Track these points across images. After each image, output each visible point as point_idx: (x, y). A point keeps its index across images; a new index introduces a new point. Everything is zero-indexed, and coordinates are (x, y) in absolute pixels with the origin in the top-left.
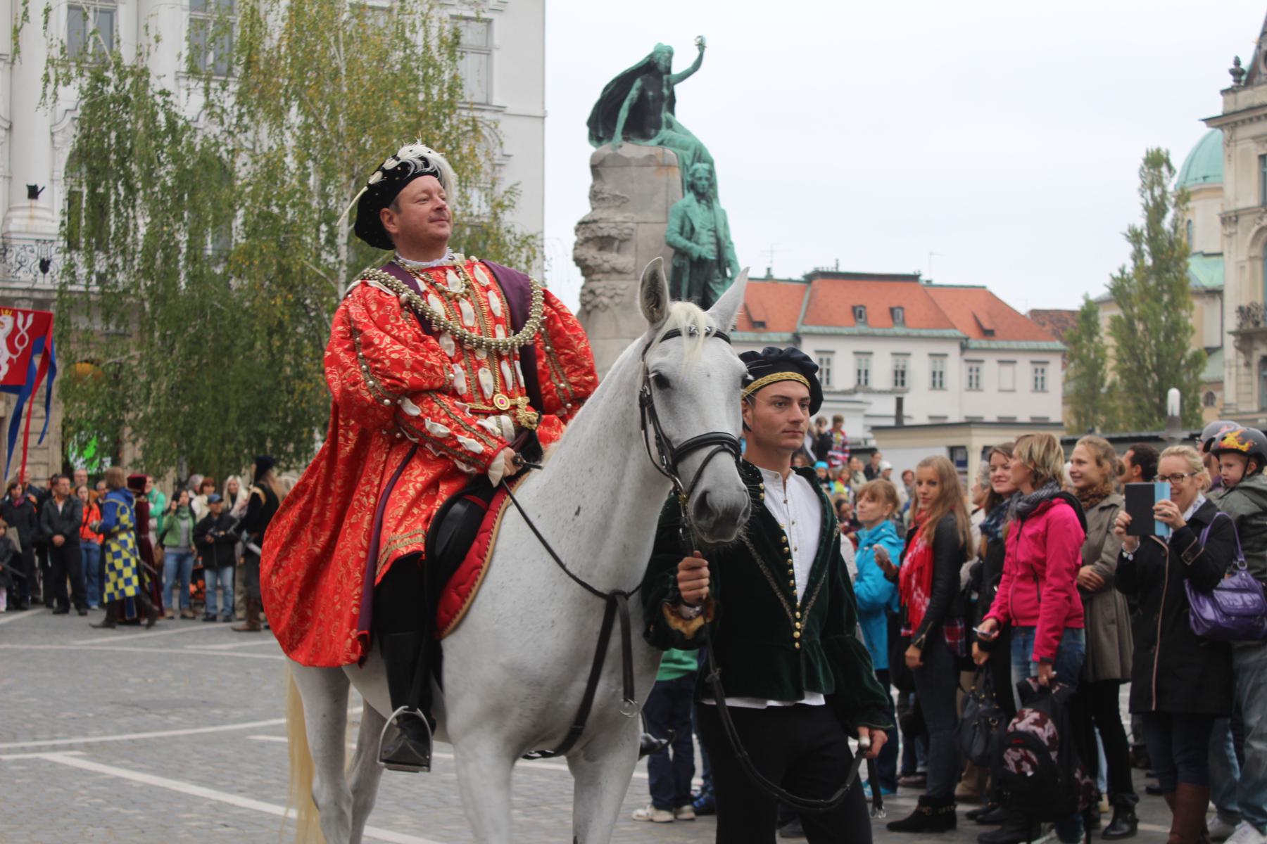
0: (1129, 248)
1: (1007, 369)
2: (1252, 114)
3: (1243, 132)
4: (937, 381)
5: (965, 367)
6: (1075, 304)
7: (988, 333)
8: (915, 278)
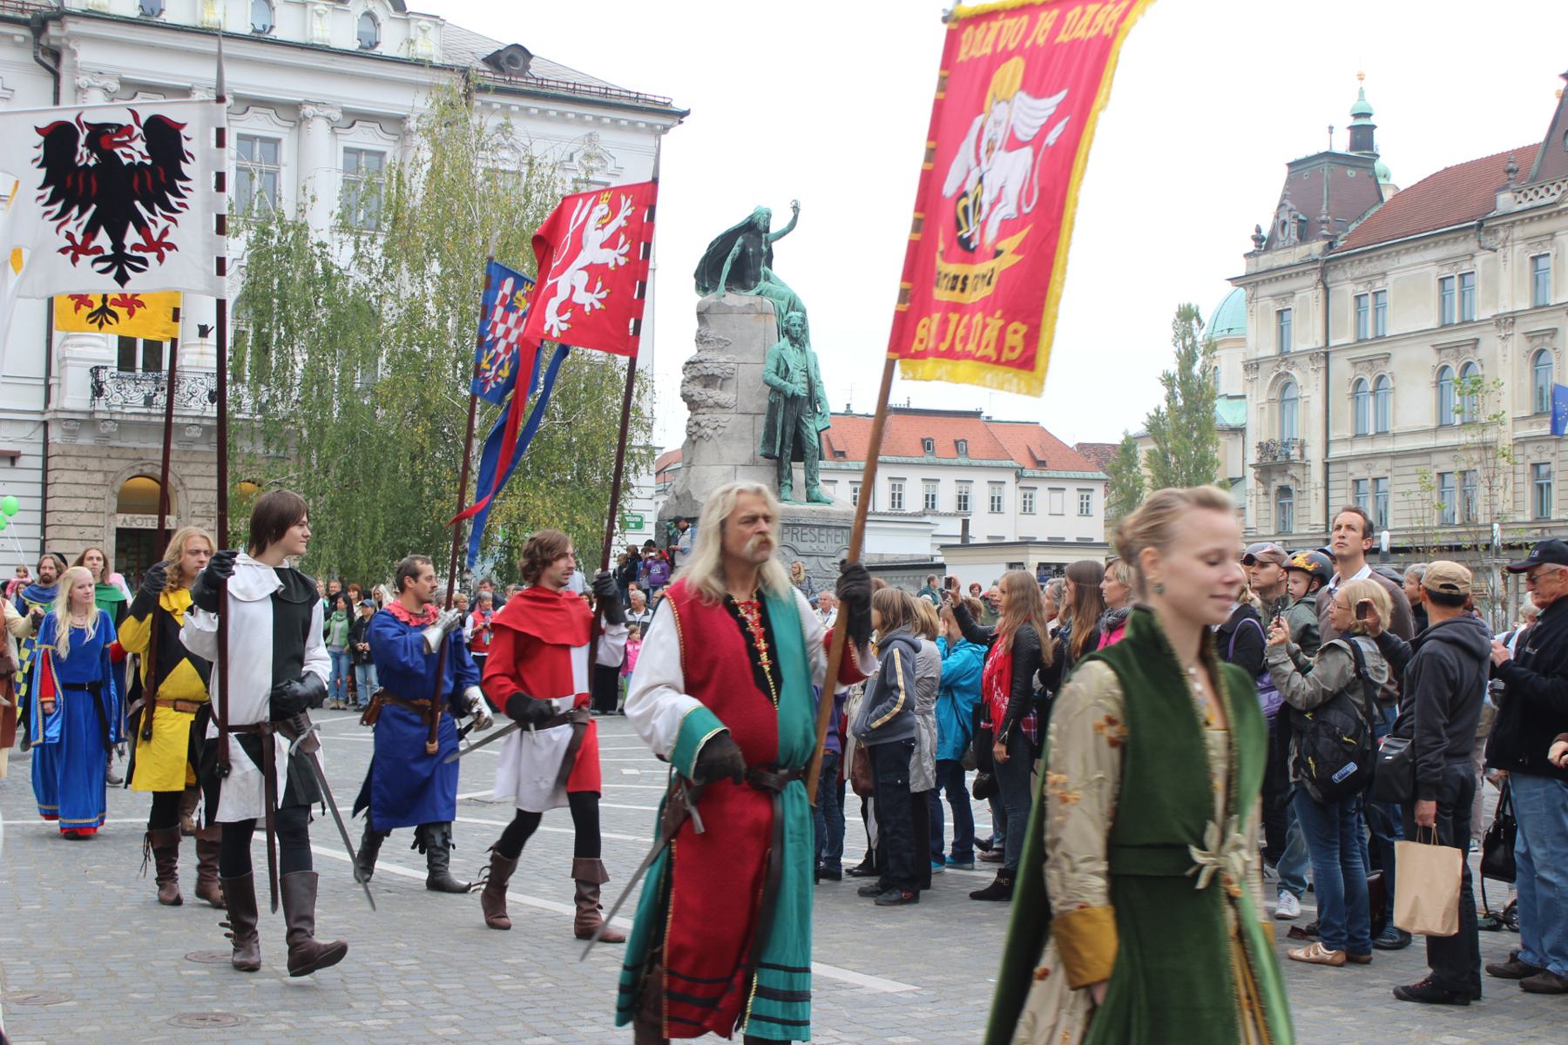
0: (1164, 391)
1: (1058, 495)
3: (1264, 291)
4: (996, 505)
5: (1020, 493)
6: (1117, 439)
7: (1041, 464)
8: (977, 414)
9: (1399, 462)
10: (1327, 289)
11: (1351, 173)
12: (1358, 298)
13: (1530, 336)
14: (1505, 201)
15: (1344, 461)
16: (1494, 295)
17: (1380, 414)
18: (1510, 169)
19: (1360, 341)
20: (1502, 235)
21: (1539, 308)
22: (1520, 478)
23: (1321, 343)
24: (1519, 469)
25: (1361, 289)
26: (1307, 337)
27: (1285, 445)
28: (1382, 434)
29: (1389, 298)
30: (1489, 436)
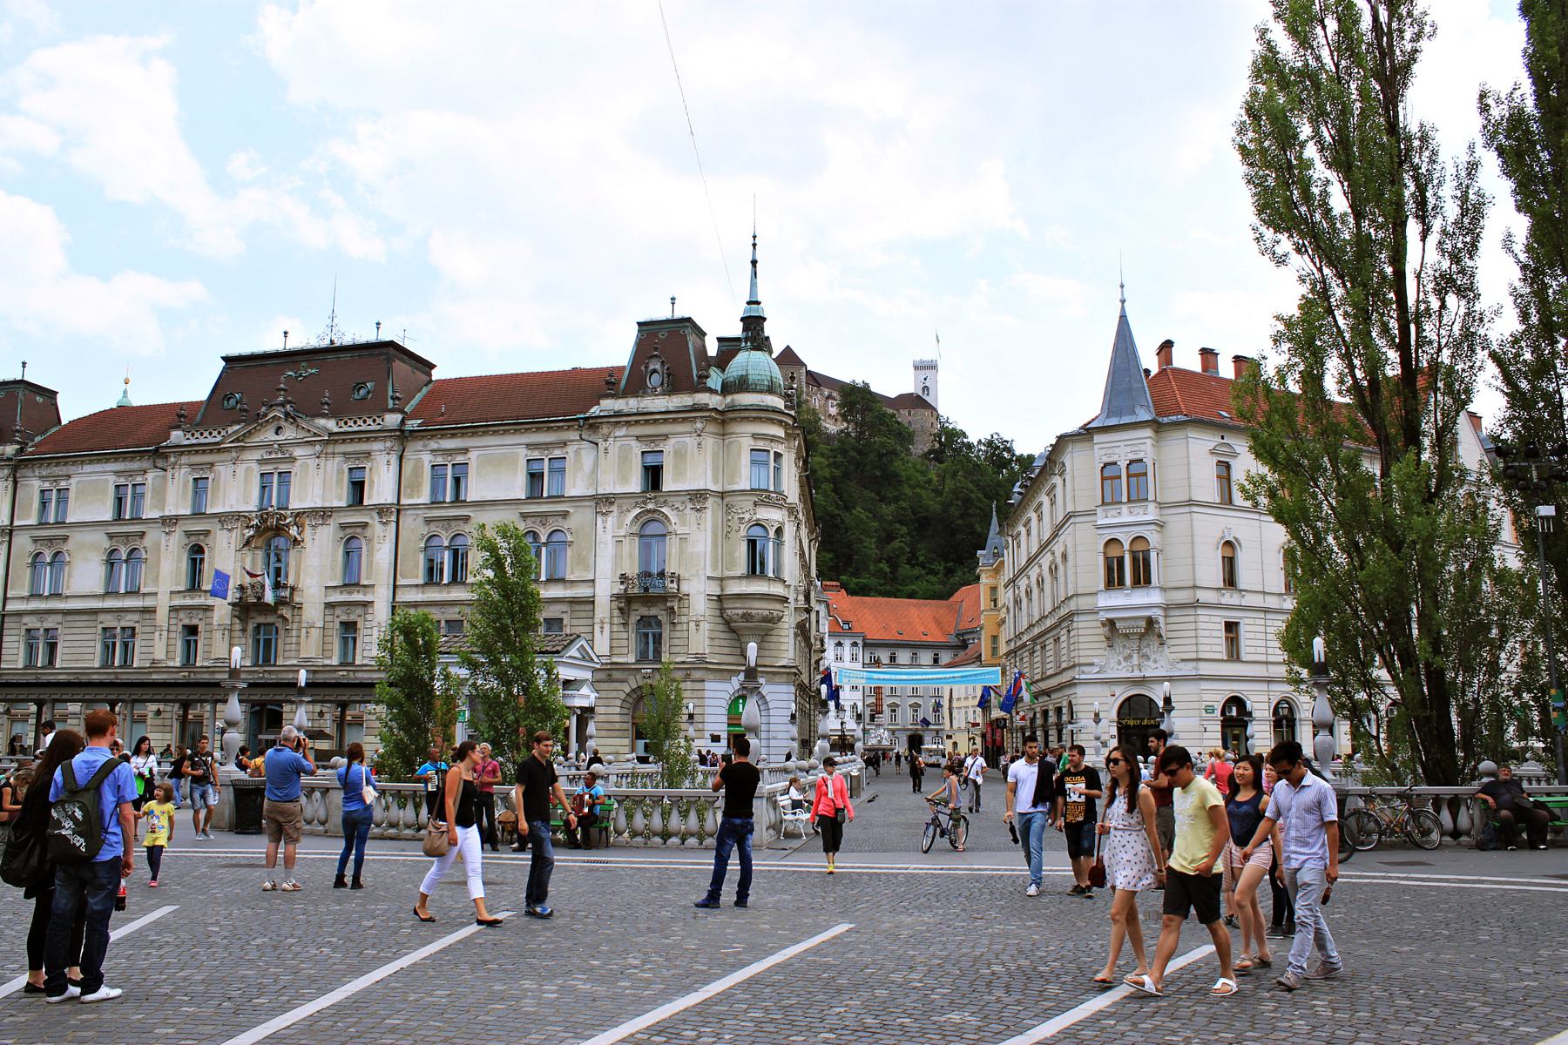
9: (69, 618)
10: (15, 482)
12: (42, 491)
14: (176, 436)
17: (55, 581)
18: (180, 415)
19: (42, 524)
20: (172, 459)
21: (198, 514)
22: (173, 635)
23: (7, 522)
24: (173, 628)
25: (47, 485)
28: (56, 595)
29: (72, 495)
30: (148, 602)
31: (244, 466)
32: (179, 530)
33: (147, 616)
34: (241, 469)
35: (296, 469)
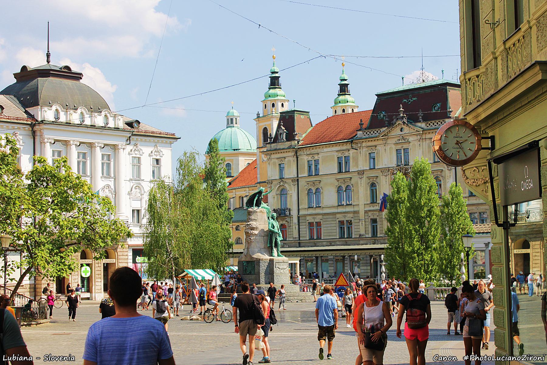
2: (276, 152)
3: (273, 156)
9: (325, 217)
10: (297, 158)
11: (302, 117)
13: (369, 178)
15: (305, 216)
16: (357, 165)
20: (359, 145)
22: (367, 223)
23: (296, 176)
24: (367, 220)
25: (310, 158)
26: (290, 172)
27: (284, 210)
29: (320, 162)
30: (356, 209)
31: (389, 147)
32: (365, 176)
33: (356, 215)
34: (387, 148)
35: (410, 146)
